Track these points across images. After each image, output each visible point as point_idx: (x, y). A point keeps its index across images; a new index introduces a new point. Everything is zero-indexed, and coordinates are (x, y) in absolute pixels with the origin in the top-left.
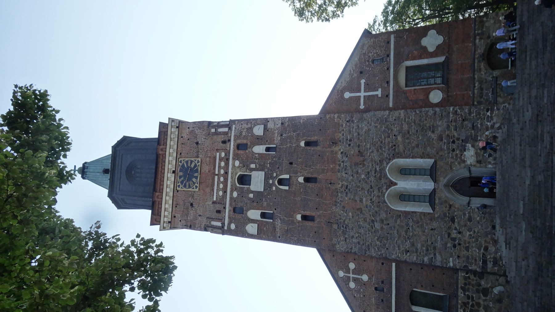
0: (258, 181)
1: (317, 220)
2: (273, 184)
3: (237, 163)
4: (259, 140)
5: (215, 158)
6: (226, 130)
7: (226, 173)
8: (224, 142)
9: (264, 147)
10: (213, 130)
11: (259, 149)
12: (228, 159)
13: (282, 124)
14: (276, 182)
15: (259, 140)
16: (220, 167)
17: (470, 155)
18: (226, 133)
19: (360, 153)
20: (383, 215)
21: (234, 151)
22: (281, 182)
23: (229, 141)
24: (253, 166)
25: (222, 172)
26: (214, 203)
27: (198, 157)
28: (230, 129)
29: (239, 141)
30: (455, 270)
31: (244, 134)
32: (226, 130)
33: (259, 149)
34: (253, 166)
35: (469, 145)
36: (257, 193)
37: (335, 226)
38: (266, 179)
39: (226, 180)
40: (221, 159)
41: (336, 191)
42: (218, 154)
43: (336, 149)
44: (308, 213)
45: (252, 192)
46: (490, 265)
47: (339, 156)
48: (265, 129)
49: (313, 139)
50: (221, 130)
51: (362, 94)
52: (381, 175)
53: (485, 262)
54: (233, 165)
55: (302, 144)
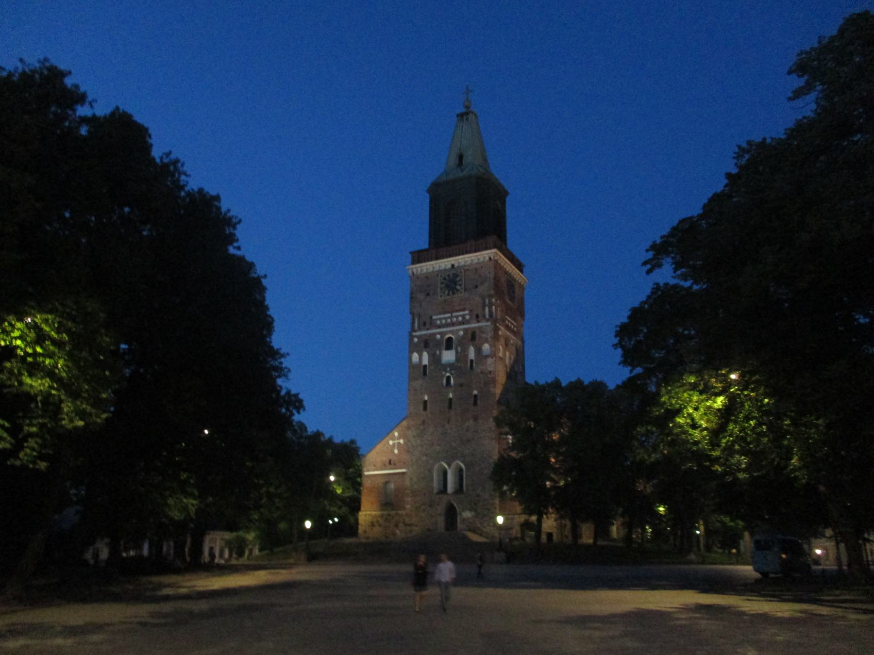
0: (448, 356)
1: (424, 413)
2: (446, 372)
3: (461, 333)
4: (478, 351)
5: (464, 310)
6: (487, 316)
7: (453, 324)
8: (477, 316)
10: (487, 301)
11: (472, 354)
12: (464, 324)
13: (490, 372)
14: (448, 374)
15: (478, 351)
16: (457, 317)
17: (467, 514)
18: (484, 316)
19: (468, 441)
20: (431, 462)
21: (469, 328)
22: (448, 378)
23: (478, 322)
24: (459, 349)
25: (455, 320)
27: (466, 290)
28: (488, 320)
29: (477, 333)
30: (405, 509)
31: (483, 335)
32: (487, 316)
33: (472, 354)
34: (459, 349)
35: (473, 513)
36: (439, 359)
37: (422, 427)
39: (447, 325)
40: (463, 316)
41: (443, 426)
42: (467, 312)
43: (471, 422)
44: (428, 405)
46: (408, 528)
47: (467, 424)
48: (487, 357)
49: (479, 402)
50: (487, 310)
52: (454, 458)
53: (410, 525)
54: (458, 331)
55: (475, 392)
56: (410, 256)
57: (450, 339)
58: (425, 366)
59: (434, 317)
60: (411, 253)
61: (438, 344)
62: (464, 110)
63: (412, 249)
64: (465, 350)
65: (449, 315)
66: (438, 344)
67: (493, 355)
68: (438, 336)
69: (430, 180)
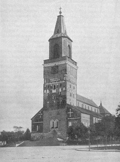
0: (54, 91)
2: (54, 95)
9: (61, 91)
11: (60, 91)
15: (62, 89)
16: (57, 79)
26: (49, 79)
34: (57, 89)
38: (54, 93)
45: (52, 90)
51: (70, 113)
56: (44, 61)
57: (55, 86)
58: (48, 93)
59: (50, 80)
60: (44, 61)
61: (51, 87)
62: (59, 14)
63: (44, 60)
64: (59, 90)
65: (54, 79)
66: (51, 87)
67: (66, 91)
68: (51, 85)
69: (49, 38)
